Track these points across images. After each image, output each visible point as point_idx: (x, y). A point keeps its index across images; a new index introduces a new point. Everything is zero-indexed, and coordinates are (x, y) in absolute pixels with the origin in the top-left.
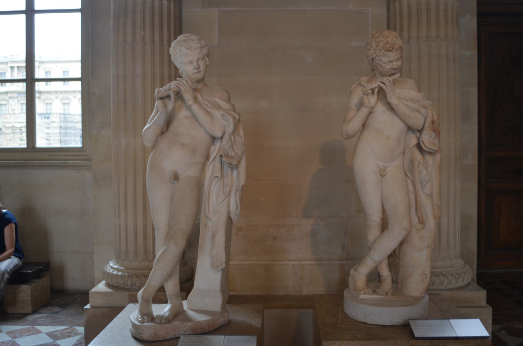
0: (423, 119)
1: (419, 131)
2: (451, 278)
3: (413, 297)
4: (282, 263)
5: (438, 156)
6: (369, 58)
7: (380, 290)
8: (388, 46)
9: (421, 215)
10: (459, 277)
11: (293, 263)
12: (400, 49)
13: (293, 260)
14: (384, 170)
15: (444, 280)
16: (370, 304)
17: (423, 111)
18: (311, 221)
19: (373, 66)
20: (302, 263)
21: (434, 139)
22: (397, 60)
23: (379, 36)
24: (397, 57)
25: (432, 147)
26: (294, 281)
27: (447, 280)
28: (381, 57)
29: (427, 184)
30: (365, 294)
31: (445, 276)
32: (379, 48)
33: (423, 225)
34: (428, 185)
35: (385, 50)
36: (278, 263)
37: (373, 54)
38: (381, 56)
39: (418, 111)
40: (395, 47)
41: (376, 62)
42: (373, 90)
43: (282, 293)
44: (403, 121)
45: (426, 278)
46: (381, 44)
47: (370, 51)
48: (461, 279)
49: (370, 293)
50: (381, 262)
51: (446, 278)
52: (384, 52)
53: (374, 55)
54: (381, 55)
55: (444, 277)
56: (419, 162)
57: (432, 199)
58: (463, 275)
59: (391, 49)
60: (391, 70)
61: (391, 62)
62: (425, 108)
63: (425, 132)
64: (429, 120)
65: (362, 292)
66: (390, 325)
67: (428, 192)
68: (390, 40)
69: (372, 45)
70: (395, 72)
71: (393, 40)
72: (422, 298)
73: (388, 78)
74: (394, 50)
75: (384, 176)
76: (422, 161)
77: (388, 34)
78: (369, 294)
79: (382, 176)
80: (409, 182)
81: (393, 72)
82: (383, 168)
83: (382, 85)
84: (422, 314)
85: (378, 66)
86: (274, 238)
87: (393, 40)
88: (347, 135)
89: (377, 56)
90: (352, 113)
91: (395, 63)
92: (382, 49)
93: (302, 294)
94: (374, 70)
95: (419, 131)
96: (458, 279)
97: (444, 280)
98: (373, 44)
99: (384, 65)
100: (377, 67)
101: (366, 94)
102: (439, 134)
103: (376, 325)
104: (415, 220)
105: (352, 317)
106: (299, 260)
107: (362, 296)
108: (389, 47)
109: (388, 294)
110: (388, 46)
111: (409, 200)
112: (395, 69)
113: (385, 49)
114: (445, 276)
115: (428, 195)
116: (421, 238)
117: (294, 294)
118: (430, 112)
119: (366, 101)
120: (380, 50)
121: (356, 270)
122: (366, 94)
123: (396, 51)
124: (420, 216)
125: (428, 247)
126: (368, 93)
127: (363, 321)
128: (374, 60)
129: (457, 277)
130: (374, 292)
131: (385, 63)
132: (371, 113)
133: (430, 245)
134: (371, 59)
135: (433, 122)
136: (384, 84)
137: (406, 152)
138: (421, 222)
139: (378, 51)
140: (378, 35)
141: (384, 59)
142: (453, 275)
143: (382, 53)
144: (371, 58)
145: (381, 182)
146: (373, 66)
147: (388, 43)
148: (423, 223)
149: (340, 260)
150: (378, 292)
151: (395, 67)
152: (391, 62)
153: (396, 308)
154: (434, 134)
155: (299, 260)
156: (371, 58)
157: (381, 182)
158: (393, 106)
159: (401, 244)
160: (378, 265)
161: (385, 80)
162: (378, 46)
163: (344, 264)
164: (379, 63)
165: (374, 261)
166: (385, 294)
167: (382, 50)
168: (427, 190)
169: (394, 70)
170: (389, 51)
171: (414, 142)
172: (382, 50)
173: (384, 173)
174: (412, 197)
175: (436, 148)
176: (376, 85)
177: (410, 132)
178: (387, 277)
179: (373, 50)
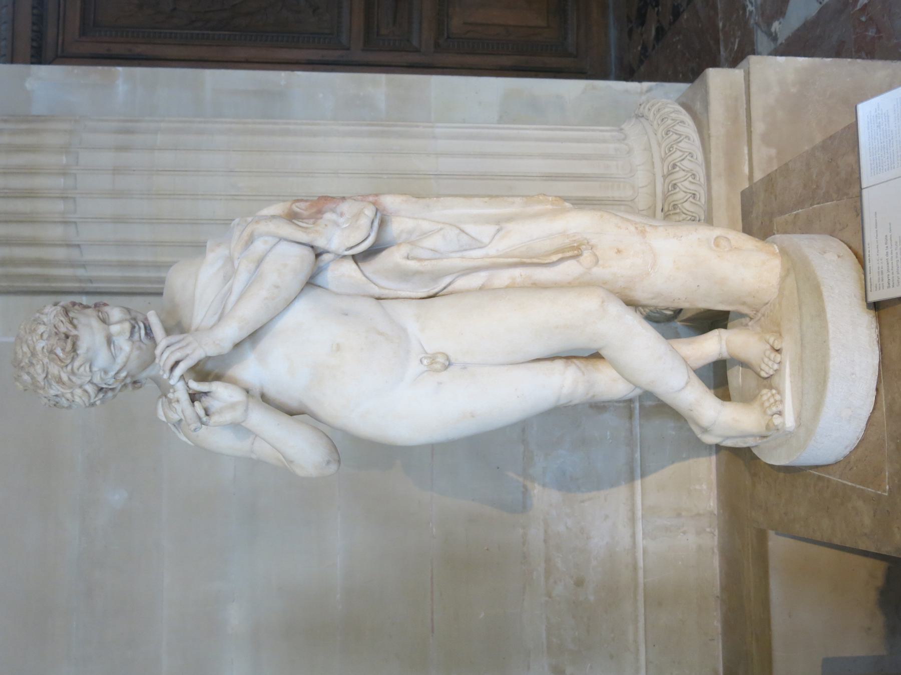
0: (284, 247)
1: (318, 256)
2: (678, 154)
3: (783, 279)
4: (641, 564)
5: (390, 202)
6: (98, 403)
7: (763, 366)
8: (59, 351)
9: (556, 252)
10: (676, 134)
11: (639, 535)
12: (71, 315)
13: (634, 536)
14: (433, 358)
15: (684, 170)
16: (818, 407)
17: (259, 246)
18: (537, 490)
19: (125, 386)
20: (639, 514)
21: (342, 215)
22: (105, 321)
23: (28, 373)
24: (95, 323)
25: (364, 222)
26: (684, 533)
27: (683, 162)
28: (95, 369)
29: (467, 234)
30: (780, 413)
31: (674, 166)
32: (65, 377)
33: (584, 247)
34: (470, 228)
35: (73, 359)
36: (641, 573)
37: (86, 391)
38: (91, 371)
39: (260, 262)
40: (63, 329)
41: (112, 381)
42: (194, 397)
43: (716, 562)
44: (289, 304)
45: (728, 240)
46: (54, 369)
47: (77, 399)
48: (677, 127)
49: (778, 397)
50: (685, 361)
51: (678, 164)
52: (77, 364)
53: (89, 388)
54: (88, 369)
55: (677, 169)
56: (408, 258)
57: (510, 219)
58: (669, 122)
59: (69, 341)
60: (136, 336)
61: (109, 341)
62: (251, 240)
63: (321, 243)
64: (288, 230)
65: (777, 420)
66: (877, 352)
67: (491, 229)
68: (41, 344)
69: (57, 396)
70: (142, 325)
71: (42, 335)
72: (784, 252)
73: (158, 352)
74: (74, 332)
75: (448, 359)
76: (404, 250)
77: (25, 349)
78: (782, 401)
79: (448, 364)
80: (462, 283)
81: (143, 332)
82: (425, 362)
83: (178, 371)
84: (839, 257)
85: (123, 374)
86: (580, 583)
87: (42, 335)
88: (328, 462)
89: (91, 382)
90: (263, 450)
91: (115, 329)
92: (69, 367)
93: (716, 512)
94: (135, 382)
95: (318, 256)
96: (680, 135)
97: (684, 170)
98: (53, 392)
99: (121, 360)
100: (126, 377)
101: (205, 419)
102: (326, 199)
103: (877, 390)
104: (569, 269)
105: (847, 452)
106: (633, 520)
107: (789, 421)
108: (63, 350)
109: (777, 347)
110: (59, 351)
111: (512, 287)
112: (133, 327)
113: (68, 361)
114: (674, 166)
115: (498, 231)
116: (619, 251)
117: (716, 533)
118: (262, 227)
119: (228, 417)
120: (73, 373)
121: (705, 430)
122: (205, 419)
123: (75, 327)
124: (560, 256)
125: (643, 233)
126: (202, 413)
127: (863, 425)
128: (104, 386)
129: (675, 137)
130: (767, 382)
131: (114, 358)
132: (265, 399)
133: (636, 228)
134: (101, 395)
135: (292, 217)
136: (177, 363)
137: (377, 291)
138: (576, 252)
139: (74, 379)
140: (26, 377)
141: (102, 358)
142: (672, 147)
143: (82, 369)
144: (96, 396)
145: (464, 367)
146: (125, 386)
147: (51, 352)
148: (578, 248)
149: (631, 417)
150: (771, 372)
151: (127, 326)
152: (109, 341)
153: (831, 335)
154: (328, 216)
155: (633, 520)
156: (96, 396)
157: (464, 367)
158: (245, 334)
159: (631, 304)
160: (691, 368)
161: (165, 359)
162: (60, 381)
163: (641, 406)
164: (112, 373)
165: (687, 384)
166: (778, 355)
167: (72, 369)
168: (484, 232)
169: (137, 329)
170: (74, 349)
171: (349, 268)
172: (72, 369)
173: (441, 359)
174: (504, 277)
175: (369, 212)
176: (180, 386)
177: (320, 280)
178: (724, 342)
179: (72, 393)
